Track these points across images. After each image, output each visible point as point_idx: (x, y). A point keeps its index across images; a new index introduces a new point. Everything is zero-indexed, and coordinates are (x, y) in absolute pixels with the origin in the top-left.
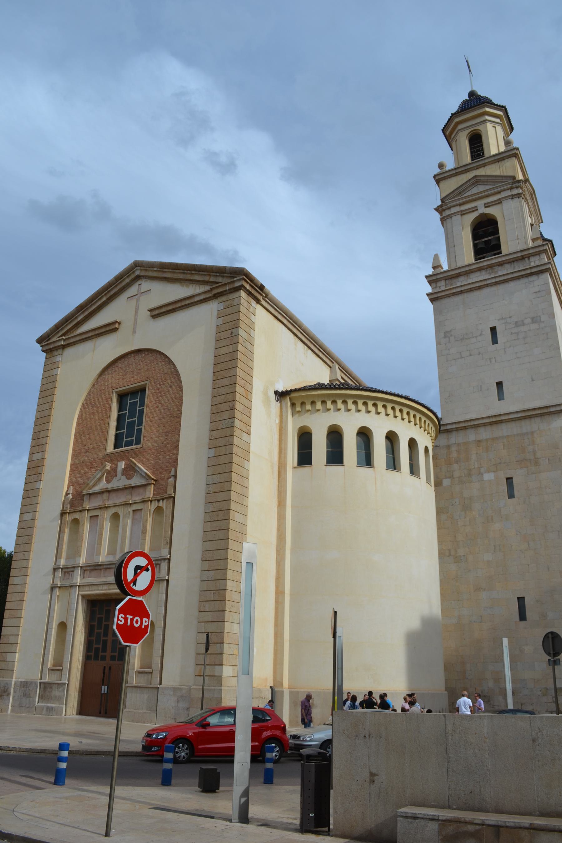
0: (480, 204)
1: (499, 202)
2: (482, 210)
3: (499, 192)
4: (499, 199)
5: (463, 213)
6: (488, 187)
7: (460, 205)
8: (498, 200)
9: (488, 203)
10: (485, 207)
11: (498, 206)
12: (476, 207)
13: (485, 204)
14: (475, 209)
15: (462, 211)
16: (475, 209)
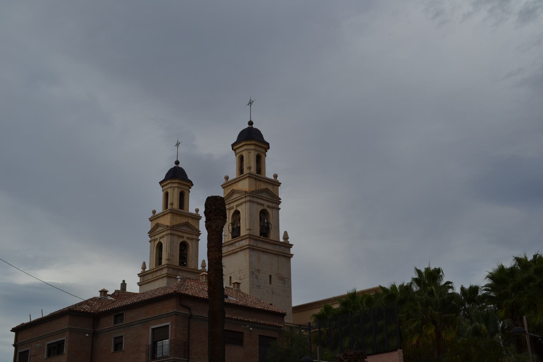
0: (266, 203)
1: (272, 208)
2: (265, 208)
3: (272, 202)
4: (273, 207)
5: (258, 204)
6: (269, 197)
7: (257, 198)
8: (272, 206)
9: (268, 205)
10: (267, 207)
11: (271, 209)
12: (264, 204)
13: (267, 205)
14: (263, 205)
15: (258, 202)
16: (263, 205)
